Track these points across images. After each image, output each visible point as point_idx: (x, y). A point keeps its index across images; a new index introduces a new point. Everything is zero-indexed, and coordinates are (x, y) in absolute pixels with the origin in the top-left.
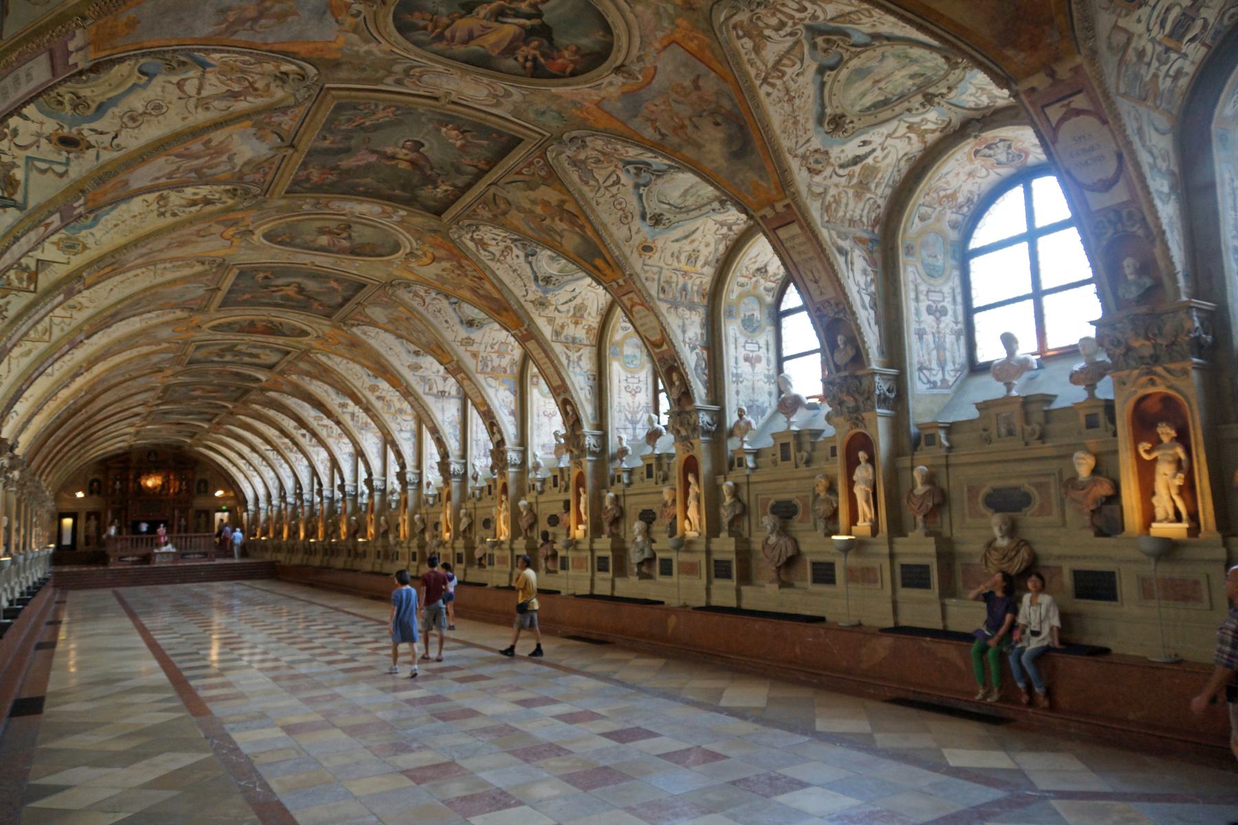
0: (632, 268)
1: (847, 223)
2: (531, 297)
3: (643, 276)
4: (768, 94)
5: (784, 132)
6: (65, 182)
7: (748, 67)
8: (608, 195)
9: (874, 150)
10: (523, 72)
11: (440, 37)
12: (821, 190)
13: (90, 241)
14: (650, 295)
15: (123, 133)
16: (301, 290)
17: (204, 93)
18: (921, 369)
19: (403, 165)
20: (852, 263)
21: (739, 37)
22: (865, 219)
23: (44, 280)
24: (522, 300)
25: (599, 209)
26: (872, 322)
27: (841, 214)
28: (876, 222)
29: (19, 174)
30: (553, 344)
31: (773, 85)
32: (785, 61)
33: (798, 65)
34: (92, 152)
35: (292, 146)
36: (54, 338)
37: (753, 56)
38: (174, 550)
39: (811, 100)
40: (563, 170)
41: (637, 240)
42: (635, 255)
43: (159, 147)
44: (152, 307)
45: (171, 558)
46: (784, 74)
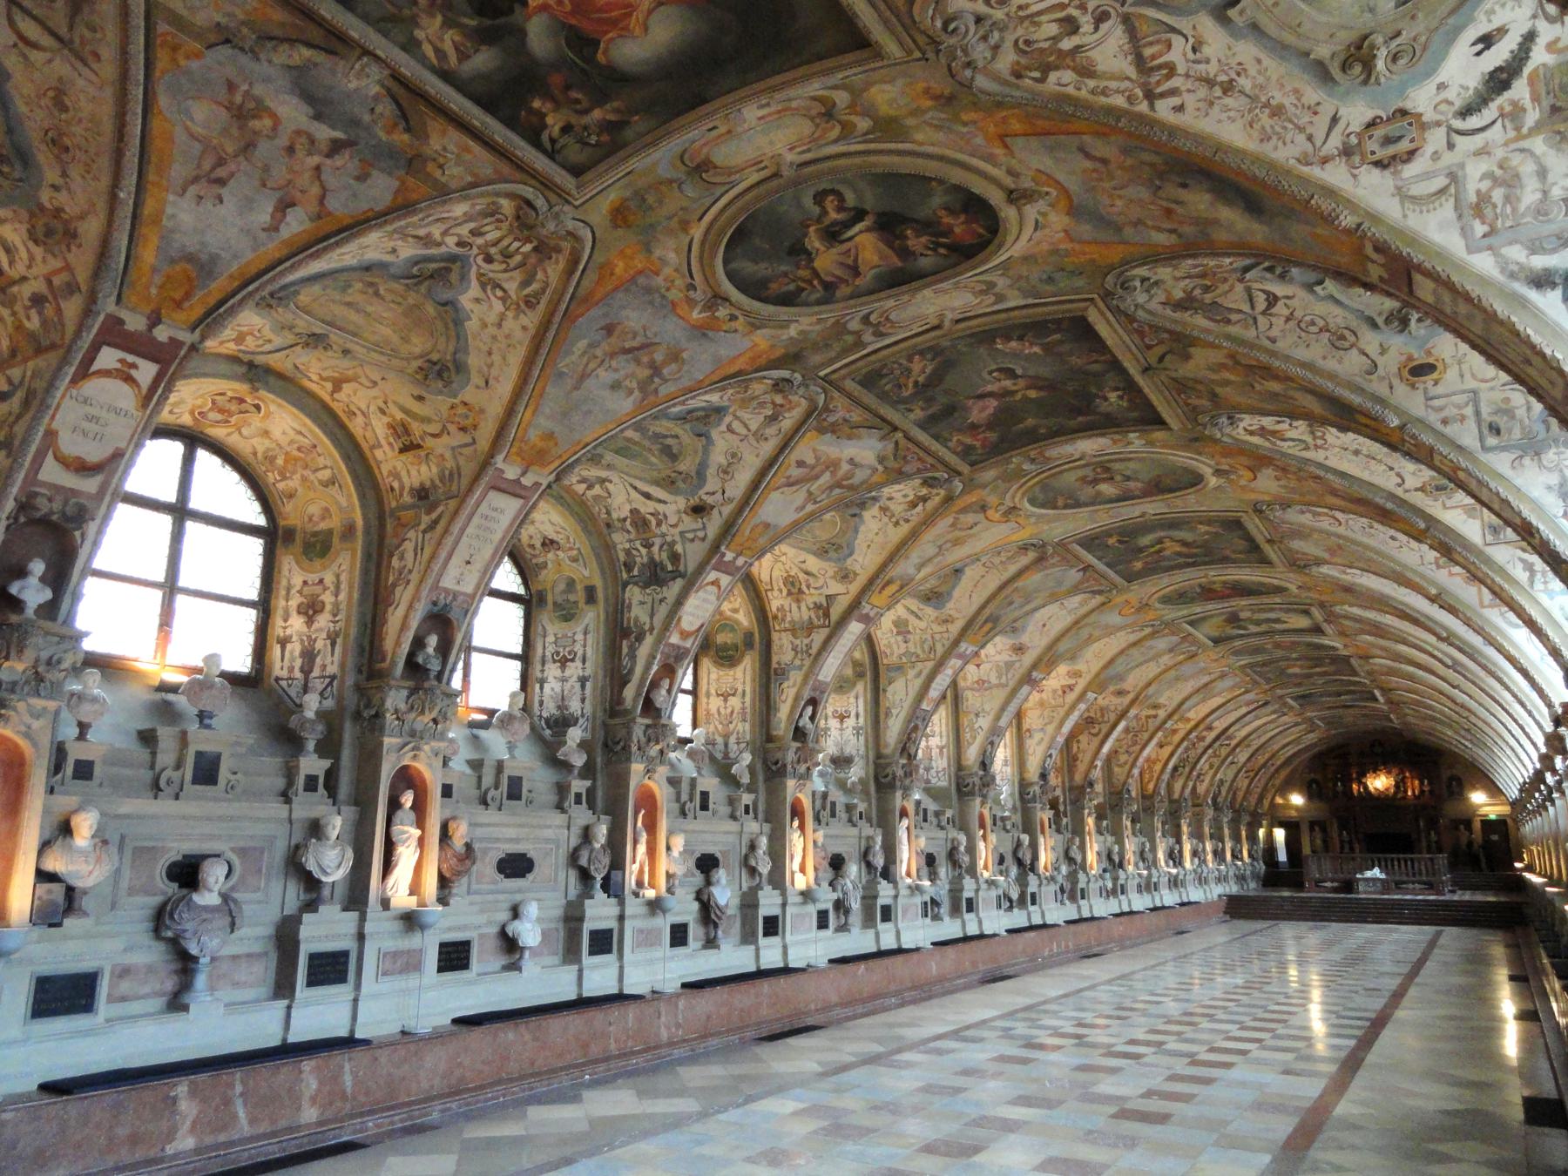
0: (1398, 411)
2: (1411, 482)
3: (1433, 419)
4: (1180, 109)
5: (1265, 138)
7: (1103, 100)
8: (1279, 322)
9: (1530, 37)
11: (829, 287)
12: (1440, 182)
13: (858, 569)
14: (1460, 448)
16: (1184, 543)
17: (754, 427)
19: (1033, 394)
21: (1042, 80)
23: (836, 612)
24: (1399, 492)
25: (1281, 345)
29: (679, 548)
30: (1489, 550)
31: (1173, 92)
32: (1148, 52)
33: (1178, 41)
34: (715, 511)
35: (895, 429)
37: (1091, 83)
38: (1383, 876)
39: (1267, 61)
41: (1390, 363)
42: (1401, 389)
46: (1171, 69)
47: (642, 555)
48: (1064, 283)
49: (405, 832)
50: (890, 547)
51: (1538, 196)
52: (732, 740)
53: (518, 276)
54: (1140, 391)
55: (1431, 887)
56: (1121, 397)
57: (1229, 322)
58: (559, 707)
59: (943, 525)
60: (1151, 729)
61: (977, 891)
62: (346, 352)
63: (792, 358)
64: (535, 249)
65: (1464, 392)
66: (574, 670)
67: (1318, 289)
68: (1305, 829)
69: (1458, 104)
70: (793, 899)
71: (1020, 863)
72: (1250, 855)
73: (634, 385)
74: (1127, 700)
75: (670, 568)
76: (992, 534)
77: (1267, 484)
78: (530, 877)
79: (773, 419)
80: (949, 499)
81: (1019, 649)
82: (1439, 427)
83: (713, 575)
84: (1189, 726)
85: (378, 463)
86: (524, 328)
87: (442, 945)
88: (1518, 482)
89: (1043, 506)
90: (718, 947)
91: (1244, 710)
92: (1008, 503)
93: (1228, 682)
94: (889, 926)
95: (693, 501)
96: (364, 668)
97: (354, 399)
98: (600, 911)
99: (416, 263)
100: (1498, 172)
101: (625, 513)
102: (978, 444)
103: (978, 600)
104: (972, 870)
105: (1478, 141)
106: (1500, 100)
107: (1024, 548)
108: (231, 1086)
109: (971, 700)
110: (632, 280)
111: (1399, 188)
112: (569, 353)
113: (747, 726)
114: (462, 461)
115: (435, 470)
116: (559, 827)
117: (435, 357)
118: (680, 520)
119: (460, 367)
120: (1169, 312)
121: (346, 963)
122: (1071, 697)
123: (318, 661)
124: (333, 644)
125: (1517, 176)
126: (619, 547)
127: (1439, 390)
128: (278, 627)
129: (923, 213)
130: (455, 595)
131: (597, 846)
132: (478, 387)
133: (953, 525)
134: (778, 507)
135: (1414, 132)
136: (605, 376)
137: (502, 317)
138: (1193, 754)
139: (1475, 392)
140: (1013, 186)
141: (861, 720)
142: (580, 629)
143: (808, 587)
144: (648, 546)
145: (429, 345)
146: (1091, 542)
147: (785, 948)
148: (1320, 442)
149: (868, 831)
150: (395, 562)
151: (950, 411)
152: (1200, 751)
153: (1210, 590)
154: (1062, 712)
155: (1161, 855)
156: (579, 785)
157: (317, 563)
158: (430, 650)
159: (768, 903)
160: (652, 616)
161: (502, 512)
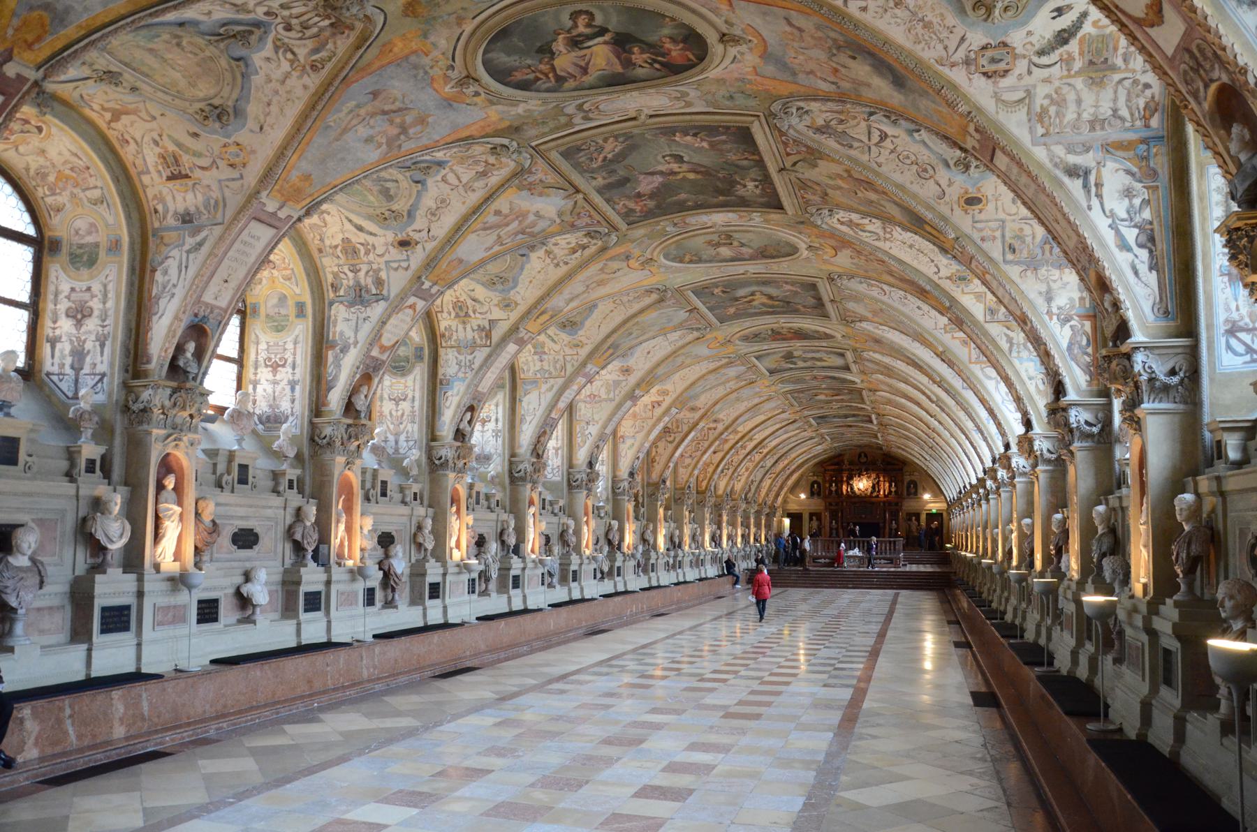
0: (956, 228)
1: (1085, 128)
2: (944, 272)
3: (976, 236)
4: (864, 9)
6: (409, 273)
8: (885, 153)
9: (1084, 15)
10: (658, 74)
11: (560, 80)
12: (1021, 94)
13: (518, 299)
14: (991, 259)
15: (432, 227)
16: (771, 297)
17: (464, 180)
18: (1232, 331)
19: (691, 176)
20: (1099, 185)
22: (1124, 112)
23: (496, 335)
24: (935, 278)
25: (884, 169)
26: (1143, 268)
27: (1070, 116)
28: (1151, 109)
29: (383, 275)
30: (987, 326)
34: (419, 246)
35: (578, 191)
36: (568, 373)
40: (813, 141)
41: (954, 193)
42: (958, 212)
43: (459, 230)
44: (651, 334)
45: (857, 562)
47: (348, 280)
48: (741, 101)
49: (169, 509)
50: (550, 283)
51: (1075, 116)
52: (402, 438)
53: (310, 44)
54: (772, 183)
55: (891, 561)
56: (757, 187)
57: (851, 147)
58: (270, 406)
59: (593, 269)
60: (711, 439)
61: (581, 564)
62: (134, 89)
63: (514, 130)
64: (332, 25)
65: (996, 220)
66: (284, 374)
67: (916, 135)
68: (806, 517)
69: (1037, 47)
70: (451, 570)
71: (610, 543)
72: (766, 539)
73: (384, 141)
74: (697, 415)
75: (374, 291)
76: (631, 278)
77: (844, 260)
78: (256, 548)
79: (483, 174)
80: (604, 249)
81: (627, 371)
82: (979, 242)
83: (412, 300)
84: (737, 437)
85: (144, 187)
86: (305, 87)
87: (200, 602)
88: (1023, 287)
89: (673, 260)
90: (396, 607)
91: (778, 426)
92: (648, 255)
93: (772, 404)
94: (518, 591)
95: (400, 237)
96: (130, 369)
97: (130, 130)
98: (312, 577)
99: (224, 25)
100: (1055, 96)
101: (338, 241)
102: (638, 208)
103: (606, 329)
104: (578, 549)
105: (1045, 73)
106: (1061, 50)
107: (650, 292)
108: (61, 709)
109: (583, 410)
110: (407, 57)
111: (996, 93)
112: (340, 111)
113: (416, 427)
114: (227, 193)
115: (200, 198)
116: (277, 508)
117: (216, 102)
118: (387, 251)
119: (238, 113)
120: (810, 133)
121: (129, 616)
122: (658, 411)
123: (88, 360)
124: (102, 346)
125: (1065, 100)
126: (328, 270)
127: (982, 217)
128: (47, 328)
129: (652, 38)
130: (213, 308)
131: (308, 524)
132: (252, 131)
133: (602, 270)
134: (473, 247)
135: (1009, 58)
136: (363, 131)
137: (287, 76)
138: (736, 459)
139: (1003, 222)
140: (726, 31)
141: (500, 424)
142: (290, 339)
143: (474, 312)
144: (355, 271)
145: (212, 92)
146: (702, 291)
147: (445, 608)
148: (888, 236)
149: (504, 516)
150: (158, 276)
151: (624, 181)
152: (741, 457)
153: (779, 333)
154: (650, 422)
155: (707, 538)
156: (292, 473)
157: (85, 272)
158: (189, 355)
159: (433, 573)
160: (356, 330)
161: (259, 238)
